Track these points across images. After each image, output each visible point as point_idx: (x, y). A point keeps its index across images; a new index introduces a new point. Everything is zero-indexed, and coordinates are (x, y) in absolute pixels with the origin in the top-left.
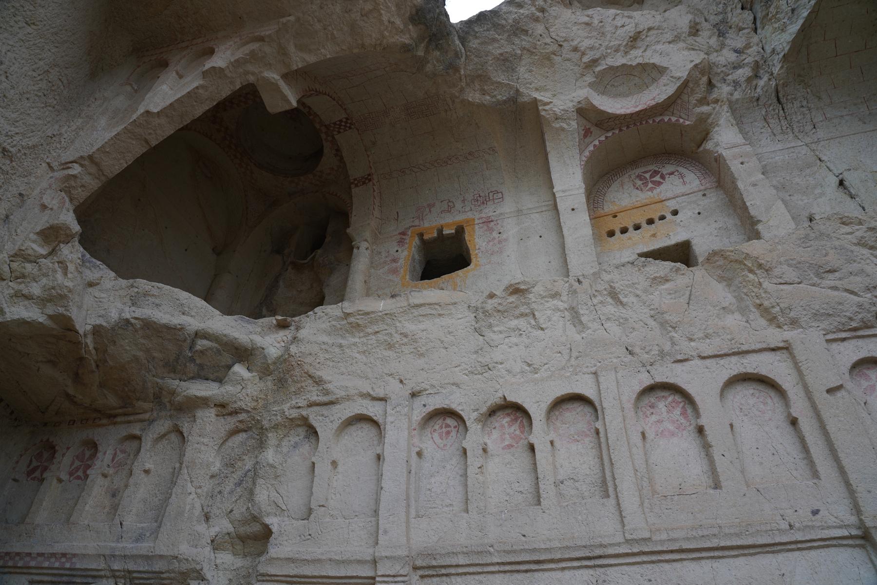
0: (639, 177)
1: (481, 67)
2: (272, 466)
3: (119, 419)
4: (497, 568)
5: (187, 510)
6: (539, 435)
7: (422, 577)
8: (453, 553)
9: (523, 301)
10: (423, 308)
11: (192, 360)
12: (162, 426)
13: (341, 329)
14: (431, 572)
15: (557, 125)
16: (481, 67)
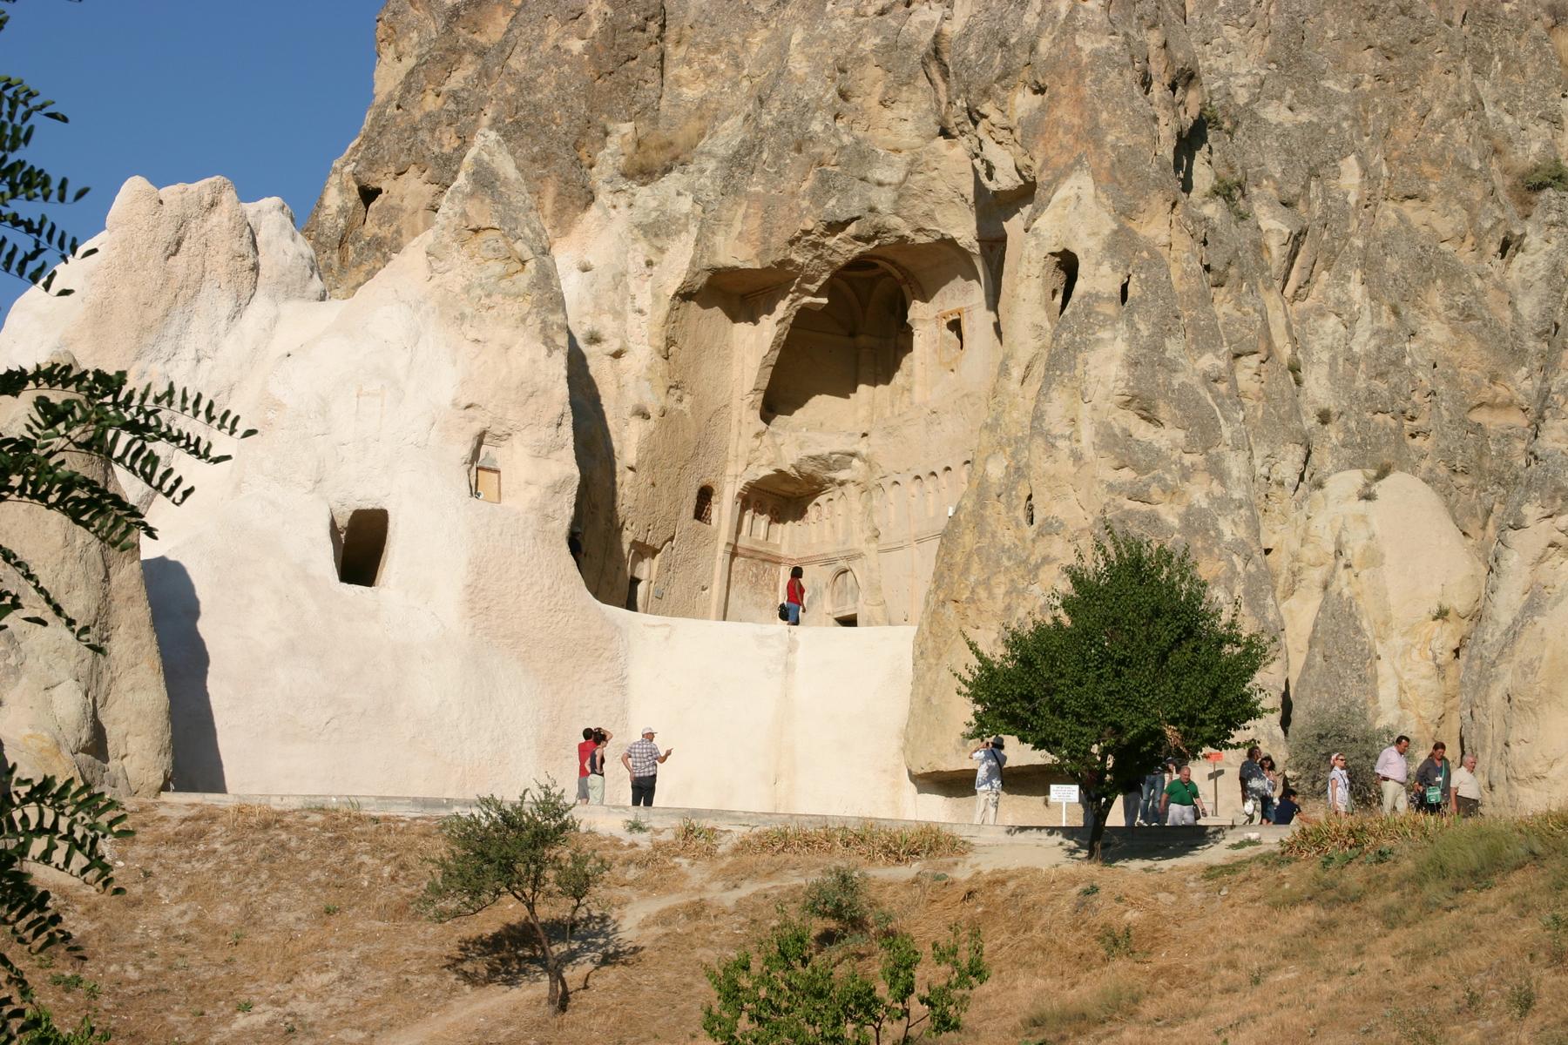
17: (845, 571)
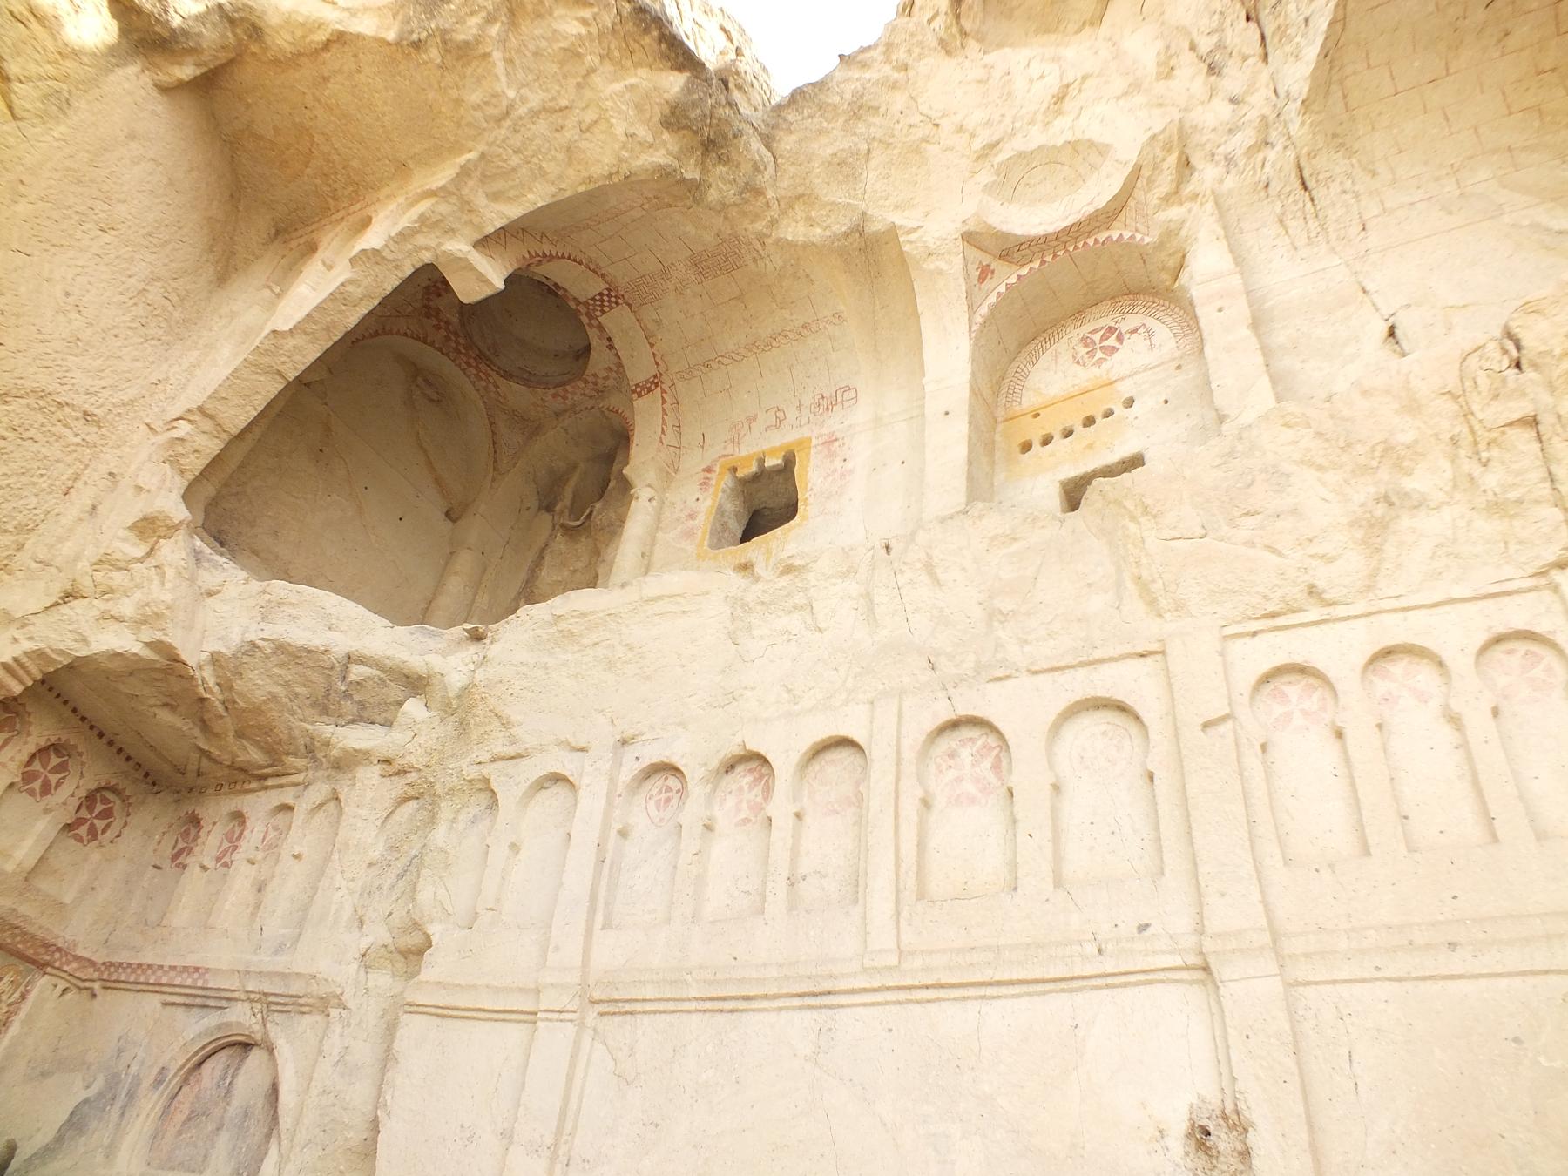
0: (1084, 341)
1: (802, 181)
2: (441, 850)
3: (270, 782)
4: (693, 1005)
5: (333, 911)
6: (780, 807)
7: (602, 1014)
8: (640, 981)
9: (799, 585)
10: (661, 602)
11: (347, 695)
12: (318, 792)
13: (548, 640)
14: (612, 1009)
15: (930, 265)
16: (802, 181)
17: (246, 1046)
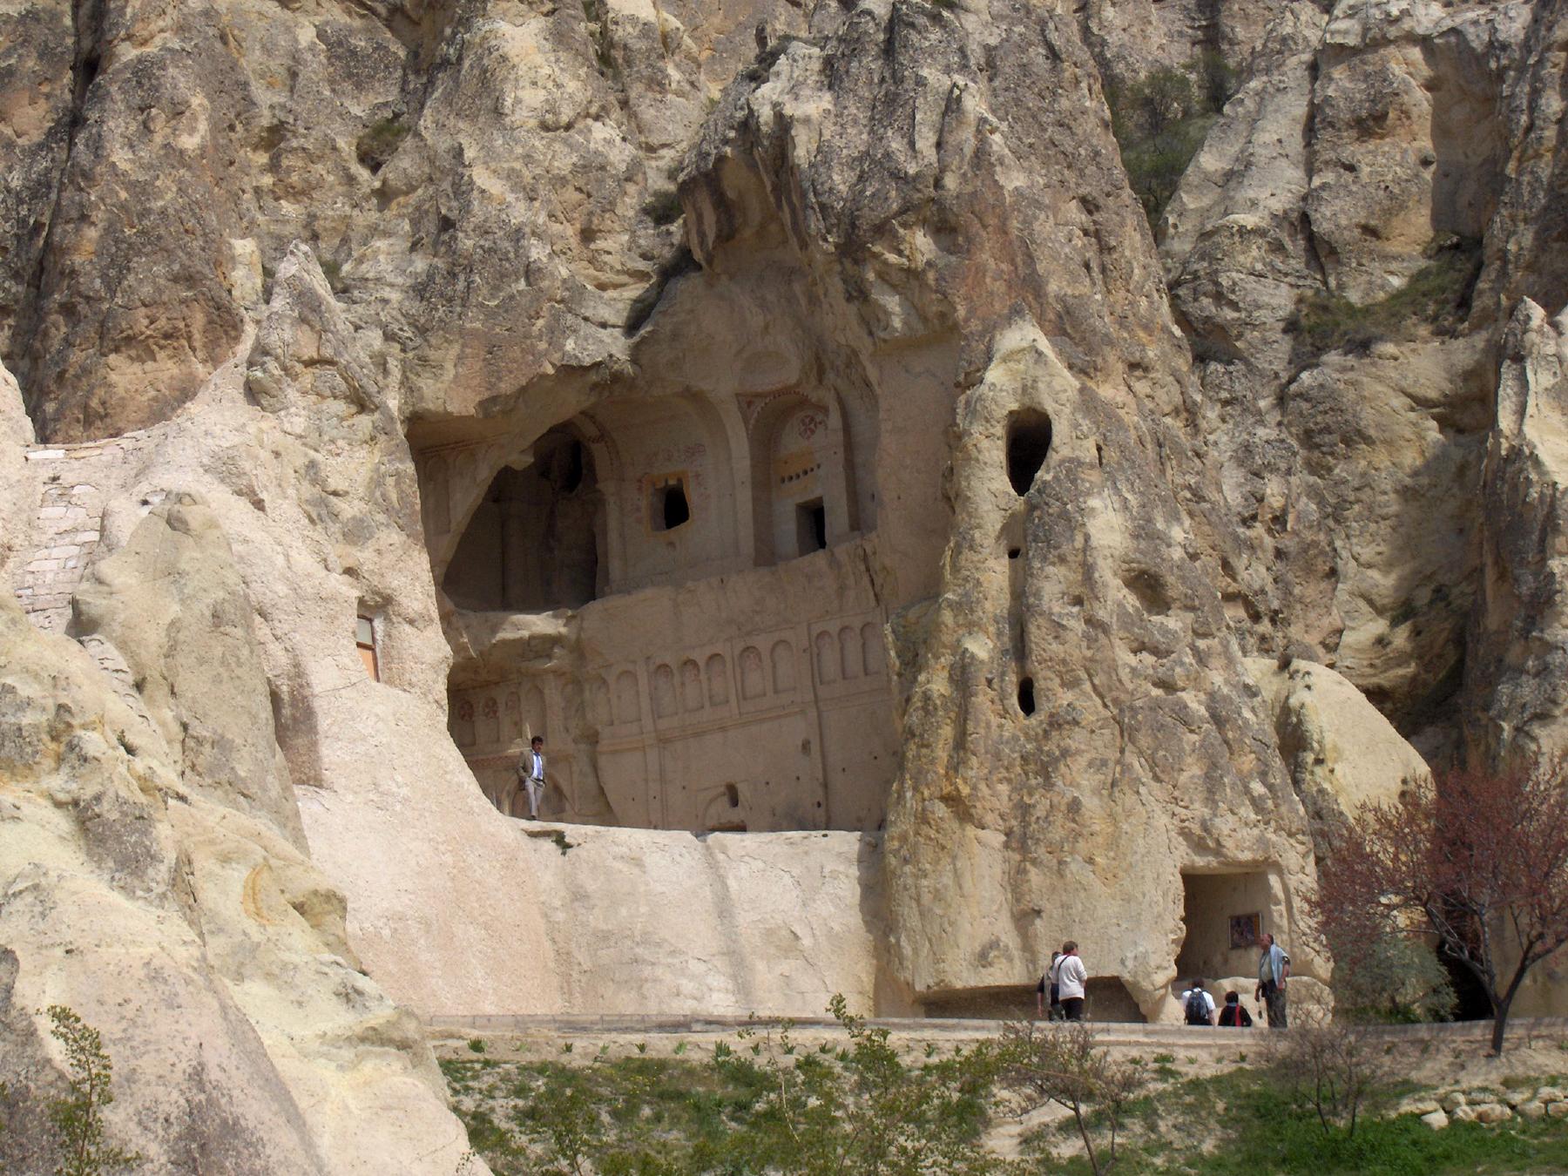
6: (703, 676)
